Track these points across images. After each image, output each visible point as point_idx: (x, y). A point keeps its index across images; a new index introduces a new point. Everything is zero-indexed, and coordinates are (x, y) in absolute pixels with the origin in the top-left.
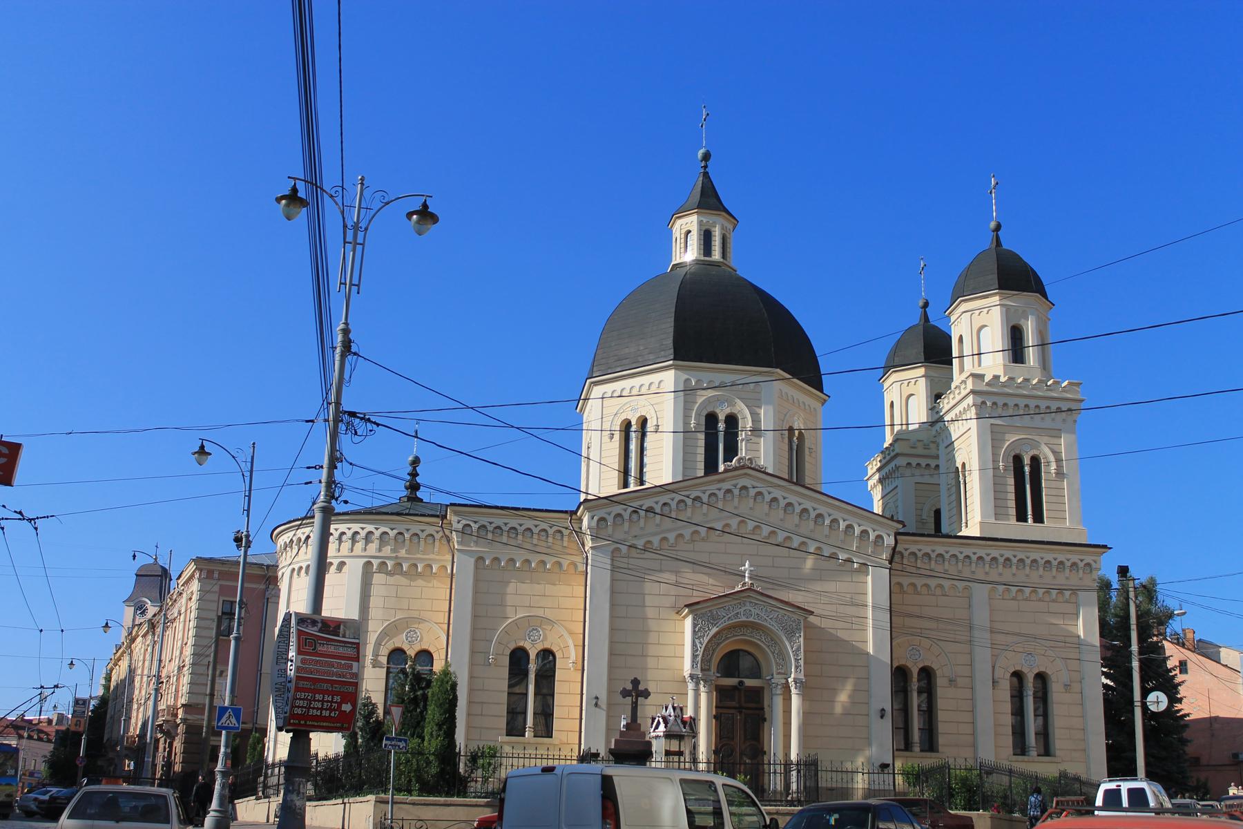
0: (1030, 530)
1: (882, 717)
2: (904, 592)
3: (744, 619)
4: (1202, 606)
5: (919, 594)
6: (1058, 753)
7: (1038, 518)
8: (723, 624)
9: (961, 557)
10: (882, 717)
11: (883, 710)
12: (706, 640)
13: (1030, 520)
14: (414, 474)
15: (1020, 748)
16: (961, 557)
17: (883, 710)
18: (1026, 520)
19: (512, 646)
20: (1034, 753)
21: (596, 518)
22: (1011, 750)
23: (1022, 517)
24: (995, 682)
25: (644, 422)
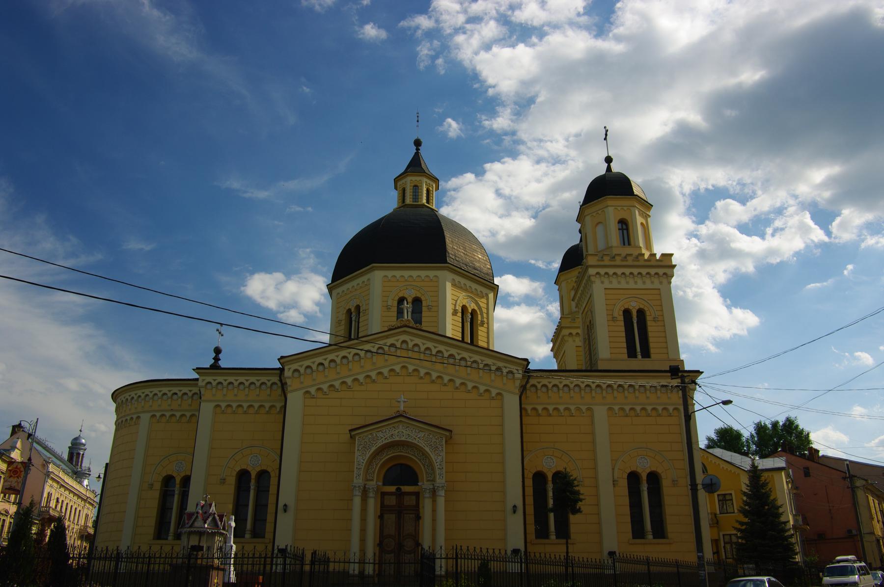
0: (639, 363)
1: (514, 512)
2: (539, 415)
3: (397, 439)
4: (745, 397)
5: (550, 415)
6: (670, 535)
7: (646, 354)
8: (380, 444)
9: (583, 386)
10: (514, 512)
11: (515, 506)
12: (368, 456)
13: (640, 357)
14: (217, 359)
15: (638, 532)
16: (583, 386)
17: (515, 506)
18: (636, 357)
19: (238, 469)
20: (650, 537)
21: (291, 370)
22: (630, 535)
23: (632, 354)
24: (615, 483)
25: (358, 308)
